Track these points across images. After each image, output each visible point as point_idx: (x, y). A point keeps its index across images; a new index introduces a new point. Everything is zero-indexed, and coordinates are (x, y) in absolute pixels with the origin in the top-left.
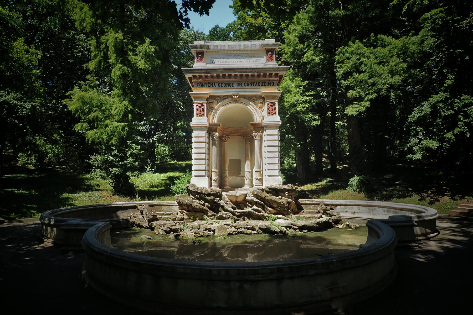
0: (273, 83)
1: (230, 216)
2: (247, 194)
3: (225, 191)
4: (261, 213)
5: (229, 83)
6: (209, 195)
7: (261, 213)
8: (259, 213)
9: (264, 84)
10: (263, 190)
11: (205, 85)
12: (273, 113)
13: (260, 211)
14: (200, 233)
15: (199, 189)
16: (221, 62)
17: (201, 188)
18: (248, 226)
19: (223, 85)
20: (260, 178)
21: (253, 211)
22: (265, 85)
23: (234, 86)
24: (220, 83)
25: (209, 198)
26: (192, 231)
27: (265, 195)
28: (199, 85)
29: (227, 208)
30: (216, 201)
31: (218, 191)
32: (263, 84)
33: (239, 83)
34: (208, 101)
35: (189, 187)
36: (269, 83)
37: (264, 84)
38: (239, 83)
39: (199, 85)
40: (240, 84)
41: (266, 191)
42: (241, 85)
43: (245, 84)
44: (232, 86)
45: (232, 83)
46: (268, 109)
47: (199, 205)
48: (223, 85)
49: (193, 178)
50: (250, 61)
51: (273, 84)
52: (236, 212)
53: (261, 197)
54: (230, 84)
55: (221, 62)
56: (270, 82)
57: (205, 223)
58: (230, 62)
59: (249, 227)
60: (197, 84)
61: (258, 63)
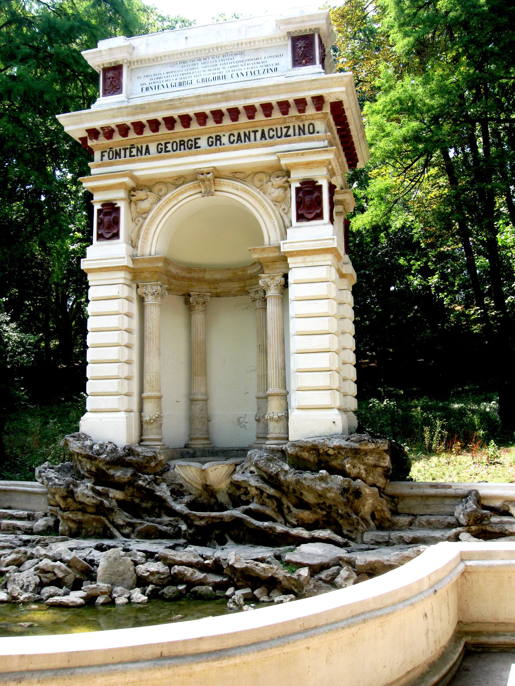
0: (311, 127)
5: (186, 140)
9: (284, 130)
11: (123, 152)
12: (312, 216)
14: (56, 571)
15: (94, 447)
16: (169, 85)
18: (205, 559)
20: (280, 415)
21: (245, 516)
22: (290, 136)
23: (199, 147)
28: (106, 154)
29: (173, 504)
30: (140, 482)
31: (150, 454)
32: (284, 133)
33: (213, 136)
34: (133, 196)
36: (299, 128)
39: (106, 154)
40: (216, 140)
42: (218, 142)
43: (232, 138)
44: (196, 148)
46: (299, 204)
47: (91, 493)
49: (87, 415)
50: (249, 74)
51: (311, 130)
52: (195, 515)
54: (190, 143)
56: (304, 125)
58: (194, 82)
59: (206, 562)
60: (102, 152)
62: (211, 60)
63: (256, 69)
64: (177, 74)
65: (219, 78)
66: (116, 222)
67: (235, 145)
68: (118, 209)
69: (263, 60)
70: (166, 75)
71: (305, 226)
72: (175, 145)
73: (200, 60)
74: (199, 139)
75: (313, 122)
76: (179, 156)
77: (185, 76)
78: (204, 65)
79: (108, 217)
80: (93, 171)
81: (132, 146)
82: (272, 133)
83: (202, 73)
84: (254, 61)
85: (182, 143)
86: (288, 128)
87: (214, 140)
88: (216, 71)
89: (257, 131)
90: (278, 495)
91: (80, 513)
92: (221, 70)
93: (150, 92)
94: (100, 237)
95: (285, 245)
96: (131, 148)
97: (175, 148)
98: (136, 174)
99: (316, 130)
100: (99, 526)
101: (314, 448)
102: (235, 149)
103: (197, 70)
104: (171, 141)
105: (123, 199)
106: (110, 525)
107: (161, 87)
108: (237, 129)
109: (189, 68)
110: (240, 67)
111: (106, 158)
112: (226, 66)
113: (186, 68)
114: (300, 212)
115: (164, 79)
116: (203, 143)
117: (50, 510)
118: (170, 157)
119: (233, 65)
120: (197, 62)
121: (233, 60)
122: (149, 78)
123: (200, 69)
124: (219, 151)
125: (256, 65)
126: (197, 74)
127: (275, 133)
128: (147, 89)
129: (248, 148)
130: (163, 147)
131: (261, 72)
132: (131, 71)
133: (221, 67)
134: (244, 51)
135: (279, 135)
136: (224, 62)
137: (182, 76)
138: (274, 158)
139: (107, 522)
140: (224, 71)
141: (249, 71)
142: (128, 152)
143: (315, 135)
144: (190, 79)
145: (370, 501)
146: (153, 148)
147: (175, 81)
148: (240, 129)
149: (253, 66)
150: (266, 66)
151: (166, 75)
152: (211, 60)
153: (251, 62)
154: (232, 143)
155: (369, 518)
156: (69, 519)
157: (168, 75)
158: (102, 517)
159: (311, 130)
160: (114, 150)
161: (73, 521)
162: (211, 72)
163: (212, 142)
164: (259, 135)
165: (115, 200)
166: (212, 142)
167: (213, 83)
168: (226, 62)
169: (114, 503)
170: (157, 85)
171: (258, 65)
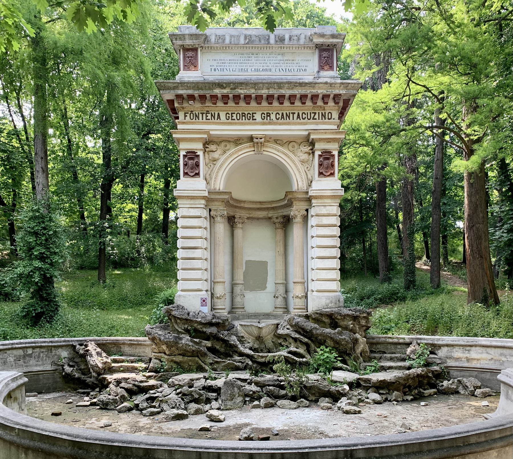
0: (330, 114)
1: (247, 363)
2: (278, 325)
3: (238, 319)
4: (304, 360)
5: (246, 113)
6: (210, 324)
7: (304, 360)
8: (301, 359)
9: (312, 115)
10: (307, 317)
11: (200, 115)
12: (329, 173)
13: (302, 356)
15: (191, 314)
16: (231, 70)
17: (195, 313)
19: (235, 117)
20: (302, 294)
21: (290, 355)
22: (316, 119)
23: (255, 119)
24: (230, 113)
25: (209, 330)
26: (178, 391)
27: (310, 325)
28: (188, 115)
33: (265, 112)
35: (171, 310)
37: (312, 115)
38: (265, 112)
39: (188, 115)
40: (267, 116)
41: (313, 319)
42: (268, 118)
43: (278, 116)
45: (253, 113)
46: (320, 165)
47: (191, 344)
48: (235, 117)
50: (287, 70)
51: (330, 117)
52: (259, 356)
53: (303, 329)
54: (249, 115)
55: (231, 70)
56: (325, 113)
57: (202, 376)
58: (249, 70)
60: (185, 113)
61: (302, 73)
62: (261, 55)
63: (292, 68)
64: (237, 62)
65: (266, 70)
66: (197, 165)
67: (279, 121)
68: (198, 156)
69: (297, 62)
70: (228, 62)
71: (324, 180)
72: (238, 115)
73: (253, 54)
74: (255, 113)
75: (331, 112)
76: (242, 124)
77: (242, 64)
78: (256, 59)
79: (192, 161)
80: (179, 127)
81: (208, 112)
82: (304, 116)
83: (255, 65)
84: (291, 62)
85: (243, 115)
86: (315, 113)
87: (266, 116)
88: (265, 65)
89: (295, 113)
90: (310, 342)
91: (181, 357)
92: (268, 64)
93: (217, 73)
94: (186, 174)
95: (312, 191)
96: (206, 113)
97: (238, 118)
98: (211, 132)
99: (333, 117)
100: (193, 364)
101: (330, 316)
102: (280, 124)
103: (251, 62)
104: (236, 113)
105: (201, 150)
106: (202, 364)
107: (225, 70)
108: (282, 110)
109: (245, 59)
110: (281, 65)
111: (188, 118)
112: (272, 62)
113: (243, 59)
114: (321, 171)
115: (227, 64)
116: (258, 117)
117: (154, 356)
118: (236, 124)
119: (276, 62)
120: (251, 55)
121: (276, 59)
122: (217, 61)
123: (253, 61)
124: (270, 124)
125: (292, 65)
126: (251, 65)
127: (306, 116)
128: (215, 70)
129: (289, 124)
130: (230, 116)
131: (296, 70)
132: (202, 53)
133: (268, 62)
134: (284, 53)
135: (309, 118)
136: (270, 59)
137: (241, 65)
138: (306, 133)
139: (200, 362)
140: (270, 65)
141: (287, 68)
142: (204, 115)
143: (332, 120)
144: (246, 68)
145: (362, 346)
146: (223, 115)
147: (235, 67)
148: (284, 110)
149: (290, 65)
150: (299, 66)
151: (228, 62)
152: (261, 55)
153: (289, 62)
154: (278, 119)
155: (359, 355)
156: (172, 361)
157: (230, 62)
158: (197, 359)
159: (330, 117)
160: (194, 112)
161: (175, 362)
162: (261, 65)
163: (264, 117)
164: (296, 116)
165: (196, 150)
166: (264, 117)
167: (262, 73)
168: (271, 59)
169: (206, 349)
170: (222, 68)
171: (294, 65)
